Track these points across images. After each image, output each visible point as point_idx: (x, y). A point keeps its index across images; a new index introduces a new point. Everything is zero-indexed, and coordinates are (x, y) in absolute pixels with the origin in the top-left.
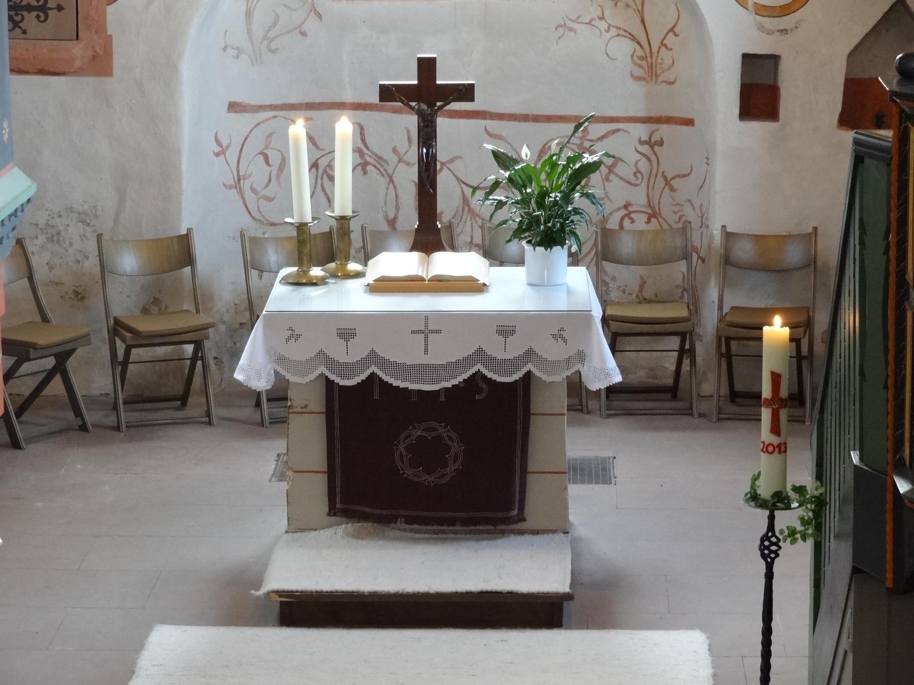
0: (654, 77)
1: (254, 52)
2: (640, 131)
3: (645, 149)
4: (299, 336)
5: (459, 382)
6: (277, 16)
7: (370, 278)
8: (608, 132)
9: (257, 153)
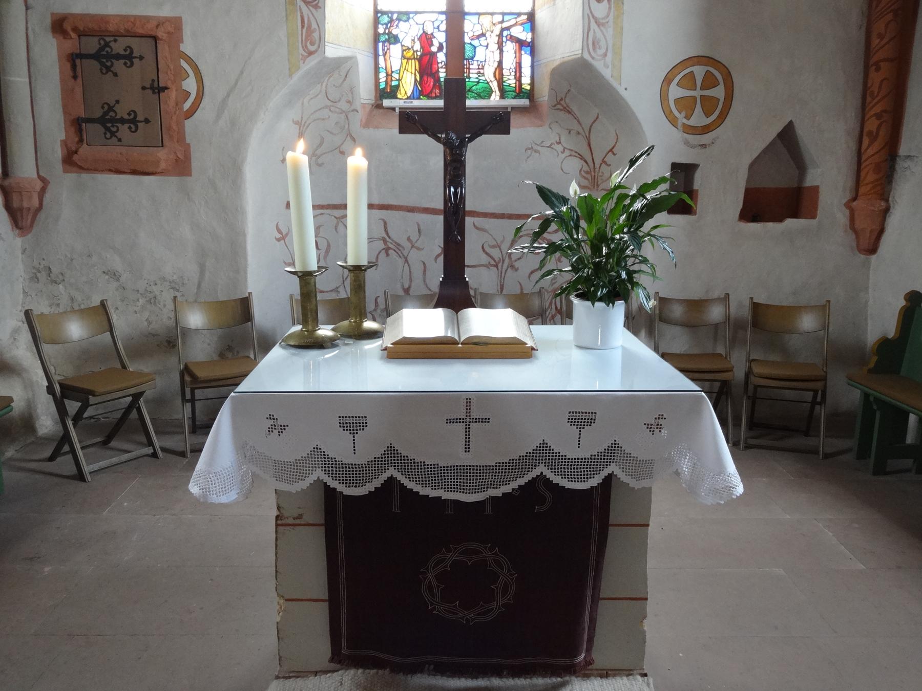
4: (283, 428)
6: (322, 139)
7: (388, 340)
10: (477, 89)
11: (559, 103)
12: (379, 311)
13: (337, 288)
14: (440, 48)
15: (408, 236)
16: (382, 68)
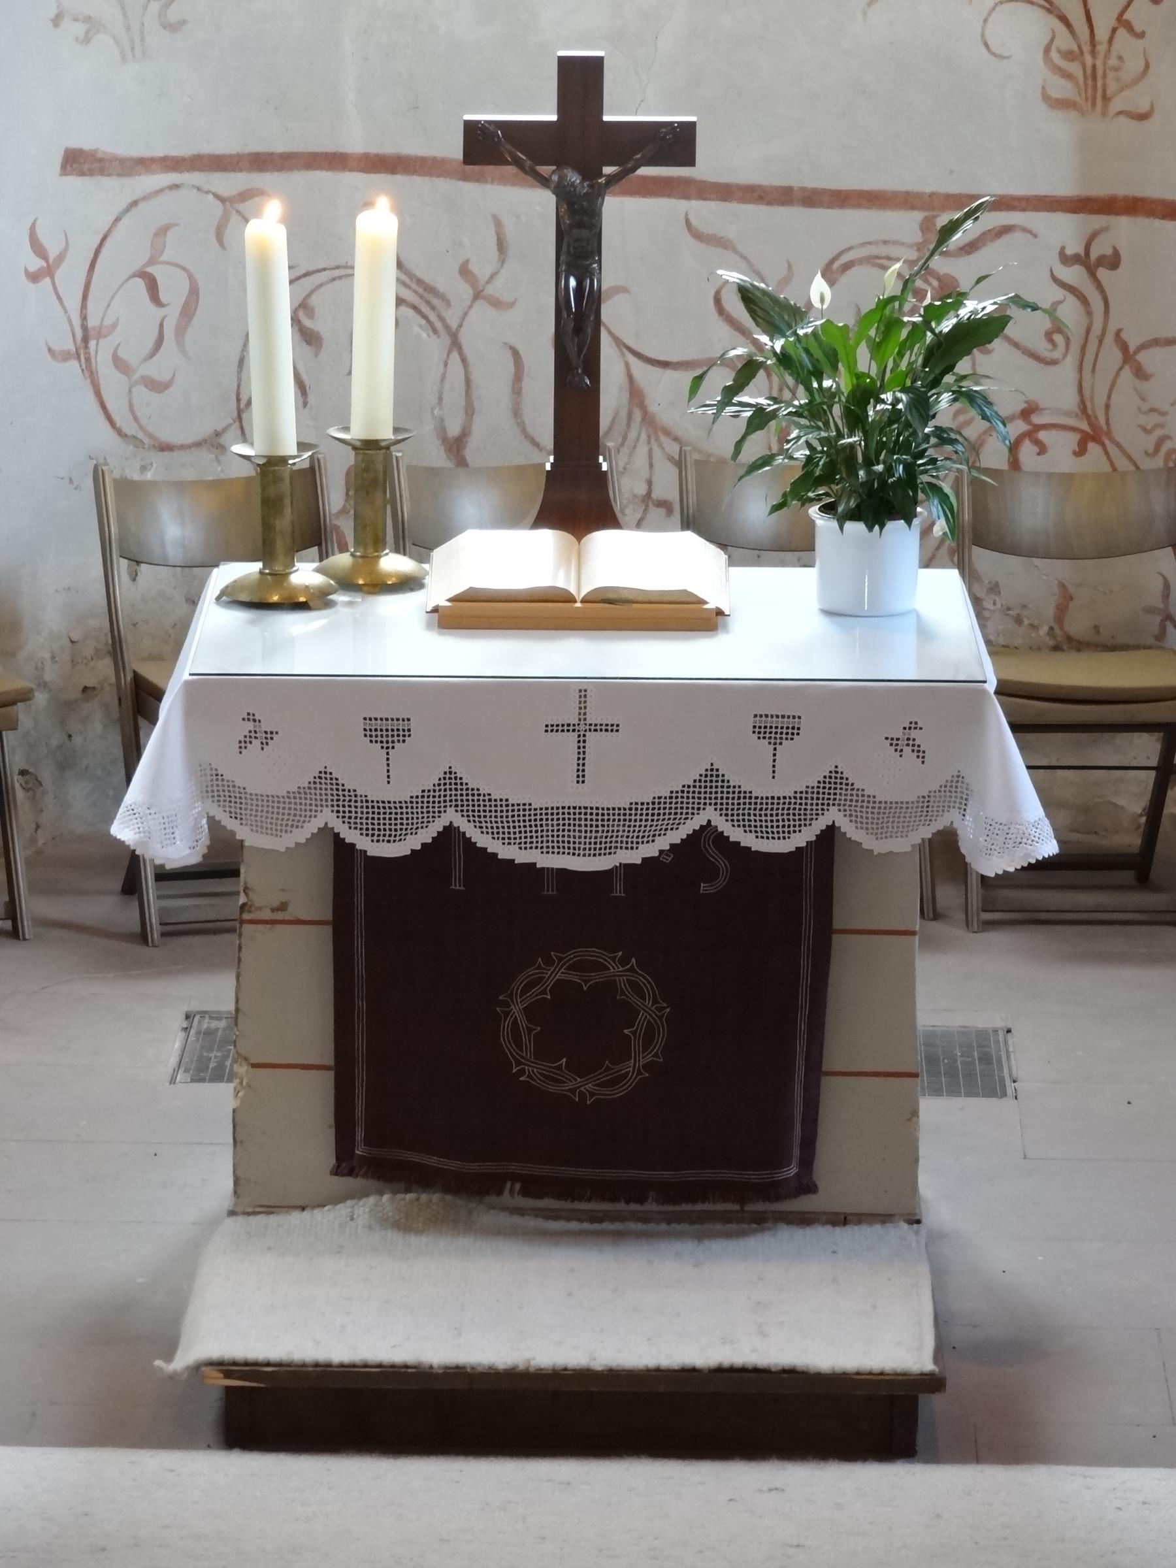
1: (128, 29)
3: (1073, 275)
4: (270, 735)
5: (661, 852)
8: (984, 234)
9: (129, 273)
13: (217, 434)
15: (461, 261)
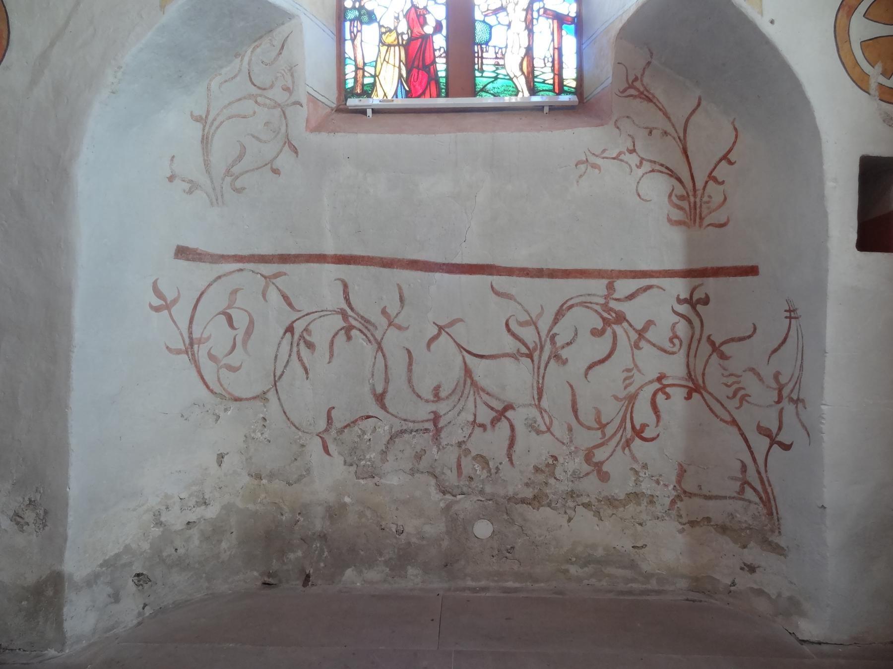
0: (698, 220)
1: (214, 189)
2: (679, 287)
3: (683, 309)
8: (638, 290)
9: (217, 313)
10: (494, 88)
11: (631, 86)
12: (333, 432)
14: (438, 28)
15: (382, 307)
16: (350, 58)
